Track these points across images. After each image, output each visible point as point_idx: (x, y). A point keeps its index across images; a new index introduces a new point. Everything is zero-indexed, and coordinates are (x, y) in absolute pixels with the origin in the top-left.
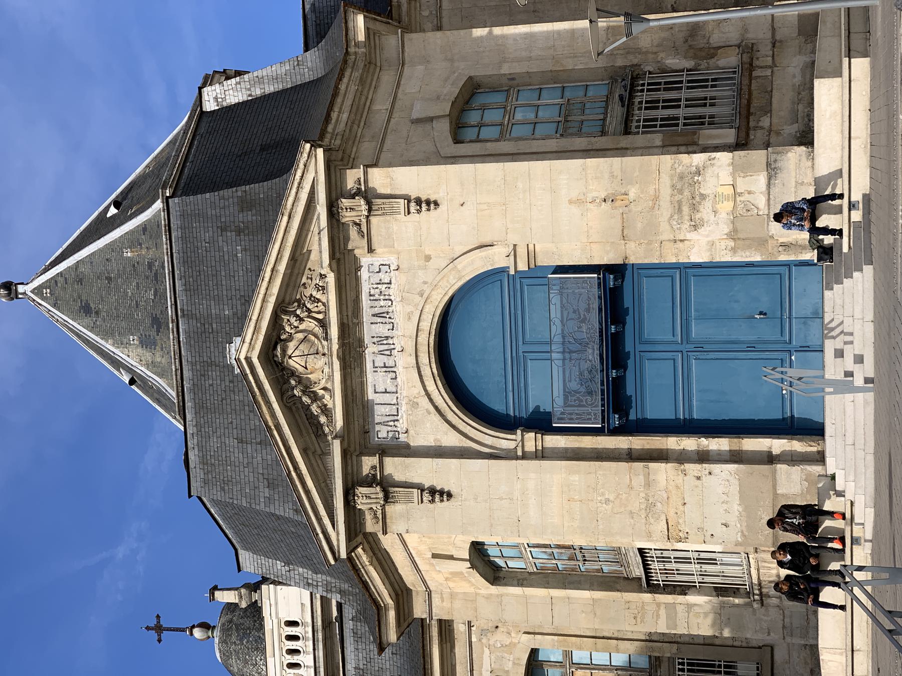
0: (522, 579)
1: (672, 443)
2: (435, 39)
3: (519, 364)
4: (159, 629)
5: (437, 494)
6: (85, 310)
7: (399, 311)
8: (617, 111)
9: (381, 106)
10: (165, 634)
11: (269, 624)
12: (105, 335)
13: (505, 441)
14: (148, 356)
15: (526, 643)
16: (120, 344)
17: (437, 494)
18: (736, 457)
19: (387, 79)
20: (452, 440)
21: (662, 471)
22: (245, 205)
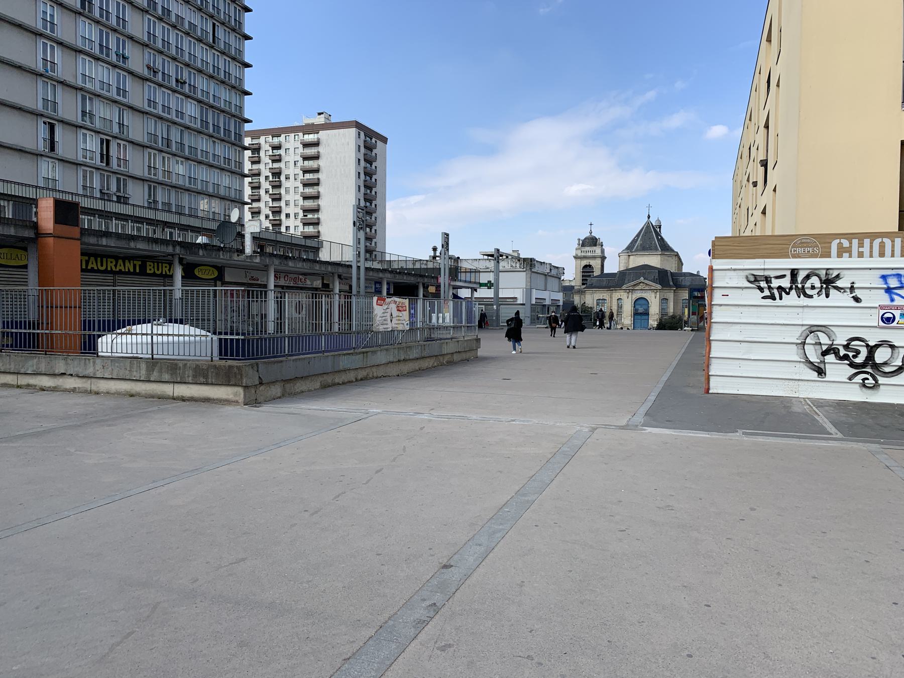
0: (618, 302)
1: (633, 318)
2: (673, 296)
3: (640, 305)
4: (591, 225)
5: (628, 297)
6: (646, 233)
7: (646, 294)
8: (664, 313)
9: (666, 291)
10: (590, 226)
11: (595, 247)
12: (642, 237)
13: (633, 304)
14: (639, 245)
15: (607, 299)
16: (641, 240)
17: (628, 297)
18: (631, 324)
19: (669, 291)
20: (633, 299)
21: (630, 317)
22: (657, 279)
